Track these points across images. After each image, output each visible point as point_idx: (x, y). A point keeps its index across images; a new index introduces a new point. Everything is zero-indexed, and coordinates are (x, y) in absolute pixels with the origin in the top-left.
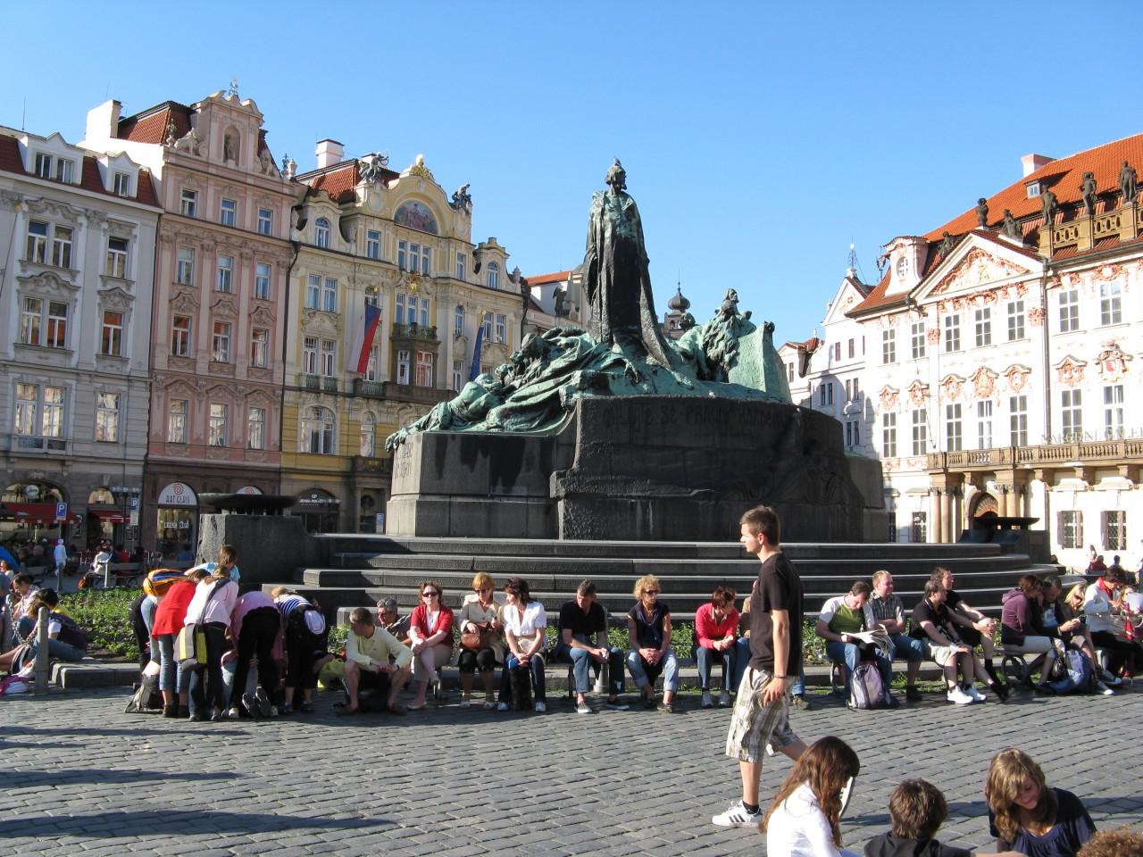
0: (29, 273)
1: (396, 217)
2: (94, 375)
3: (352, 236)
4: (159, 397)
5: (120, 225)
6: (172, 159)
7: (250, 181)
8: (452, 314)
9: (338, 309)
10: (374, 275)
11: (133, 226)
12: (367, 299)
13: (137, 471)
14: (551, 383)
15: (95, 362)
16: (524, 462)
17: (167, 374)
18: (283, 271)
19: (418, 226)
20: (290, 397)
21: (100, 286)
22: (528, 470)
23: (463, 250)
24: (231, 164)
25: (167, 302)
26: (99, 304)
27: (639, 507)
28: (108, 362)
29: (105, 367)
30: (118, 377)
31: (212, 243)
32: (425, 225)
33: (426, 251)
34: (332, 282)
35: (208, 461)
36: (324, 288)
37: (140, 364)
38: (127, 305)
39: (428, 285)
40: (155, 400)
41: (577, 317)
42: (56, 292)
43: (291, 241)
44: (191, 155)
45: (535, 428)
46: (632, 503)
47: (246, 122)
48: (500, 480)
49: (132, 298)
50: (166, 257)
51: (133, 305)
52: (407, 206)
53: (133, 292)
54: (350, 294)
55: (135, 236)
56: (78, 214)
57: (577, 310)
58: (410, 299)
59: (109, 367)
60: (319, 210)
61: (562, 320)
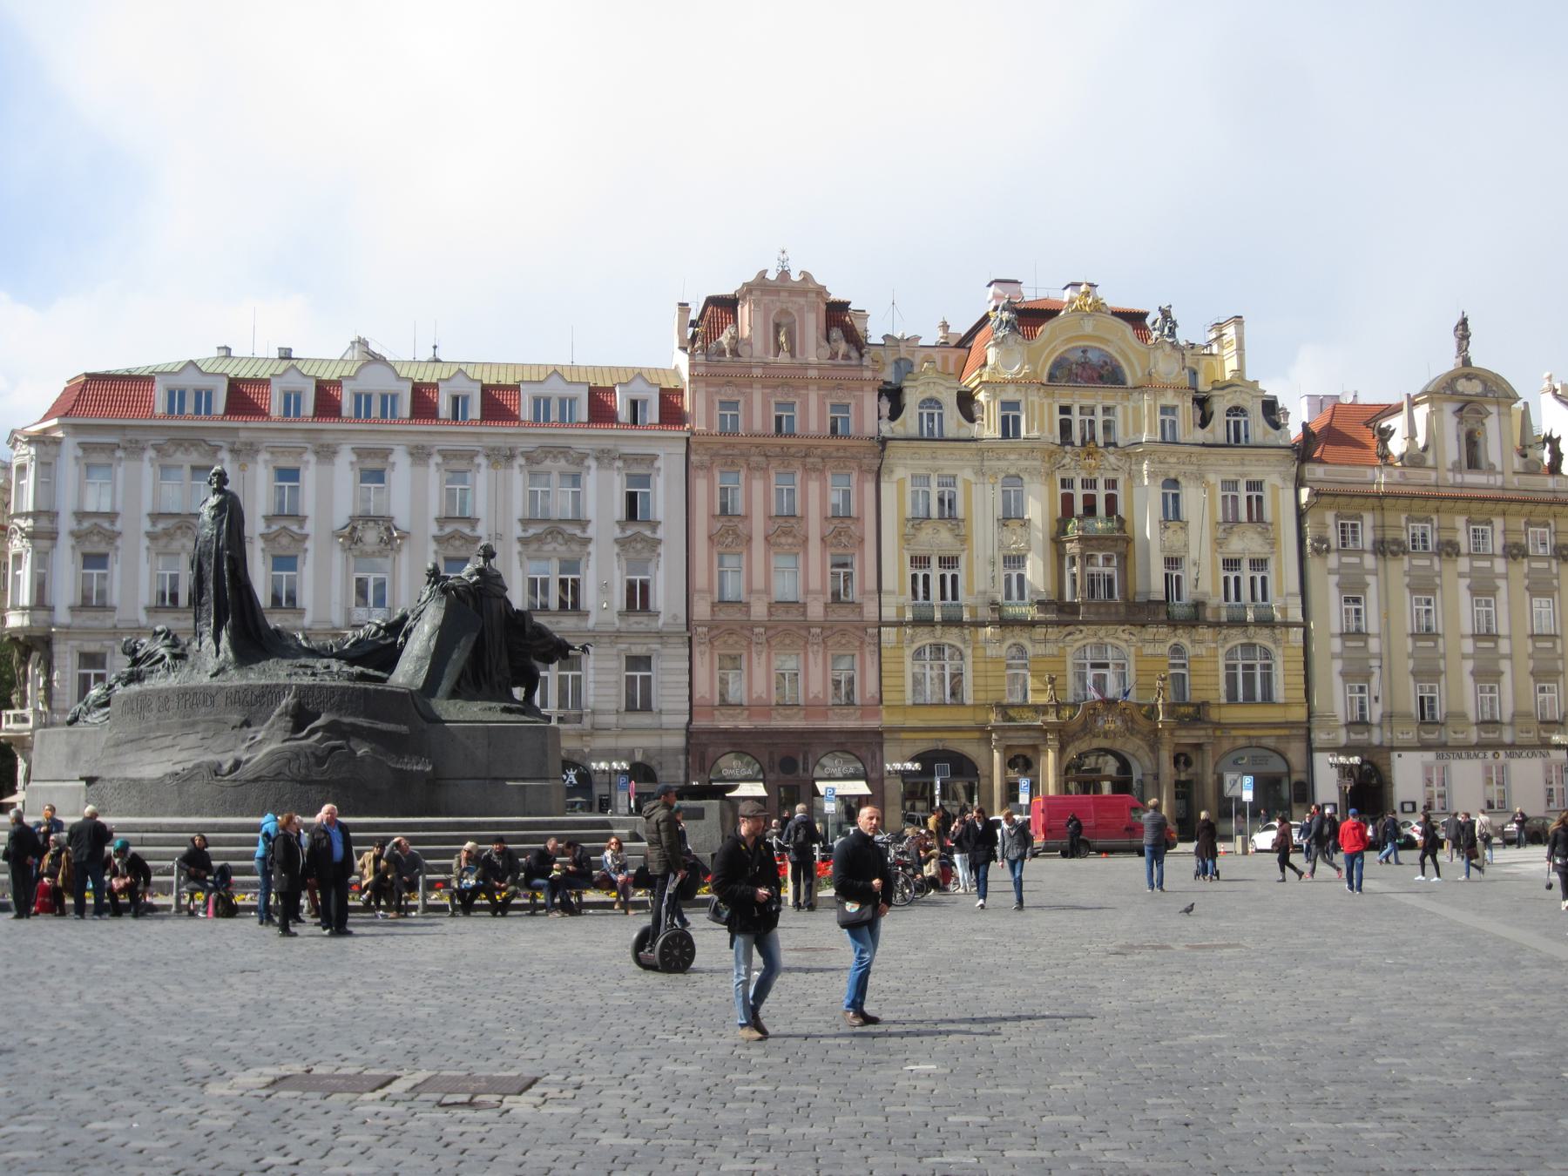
0: (531, 532)
1: (1051, 377)
2: (617, 635)
3: (978, 415)
4: (702, 654)
6: (701, 370)
7: (813, 373)
9: (960, 511)
10: (1012, 463)
11: (654, 457)
13: (679, 741)
15: (616, 621)
17: (713, 626)
18: (871, 478)
19: (1091, 380)
20: (889, 634)
21: (617, 533)
24: (784, 357)
28: (633, 619)
30: (647, 634)
31: (761, 459)
32: (1108, 375)
33: (1106, 410)
37: (675, 617)
39: (1112, 459)
42: (564, 548)
47: (802, 301)
50: (701, 486)
51: (662, 549)
53: (660, 533)
54: (977, 491)
56: (583, 457)
59: (638, 622)
60: (921, 389)
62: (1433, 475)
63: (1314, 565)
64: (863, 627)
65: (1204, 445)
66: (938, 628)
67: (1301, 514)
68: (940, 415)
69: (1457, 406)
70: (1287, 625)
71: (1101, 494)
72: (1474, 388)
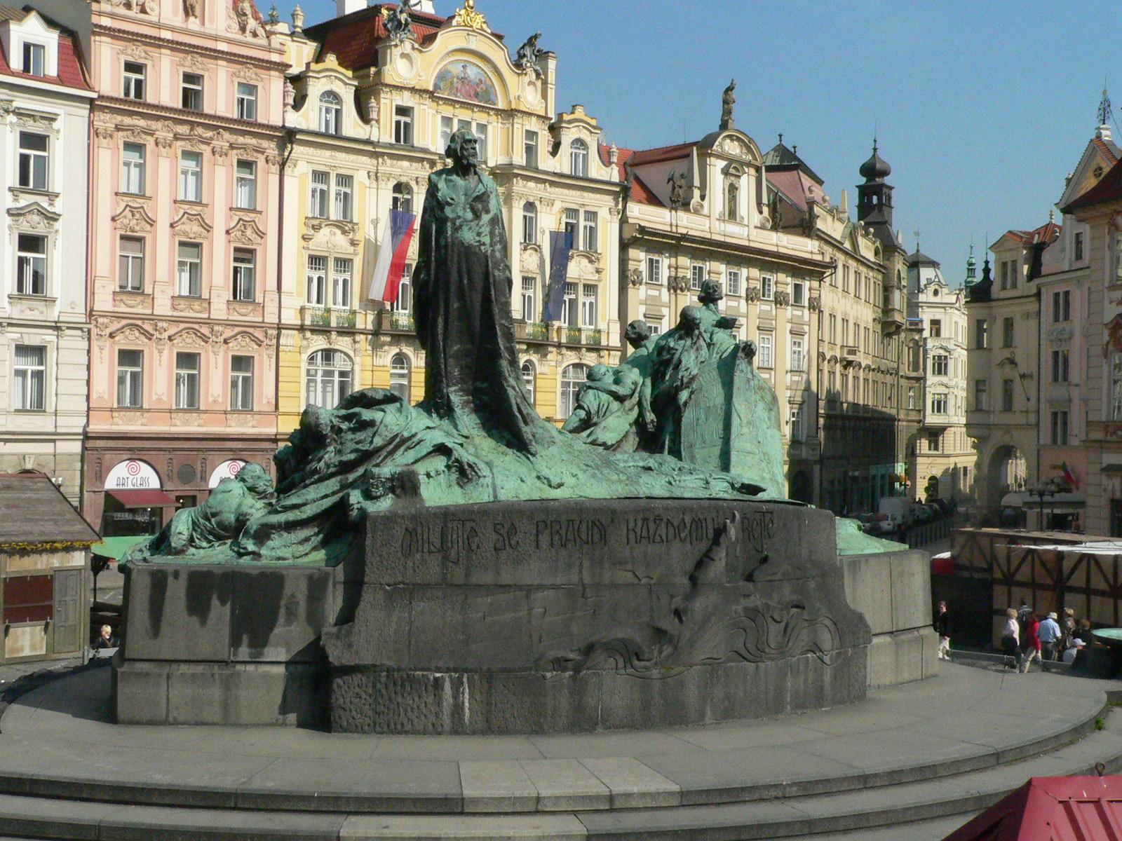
1: (436, 86)
3: (374, 115)
5: (31, 115)
6: (105, 22)
7: (222, 46)
11: (51, 119)
12: (395, 200)
13: (76, 447)
14: (333, 484)
16: (282, 611)
18: (275, 169)
20: (290, 339)
21: (9, 201)
22: (289, 622)
23: (533, 124)
24: (193, 23)
26: (10, 227)
27: (447, 685)
28: (26, 304)
29: (22, 311)
34: (345, 180)
35: (174, 429)
36: (333, 188)
40: (95, 350)
41: (702, 206)
44: (134, 13)
45: (306, 554)
46: (436, 679)
48: (245, 638)
49: (52, 218)
50: (105, 157)
51: (57, 225)
52: (450, 68)
53: (58, 207)
55: (58, 131)
57: (703, 197)
61: (681, 214)
63: (631, 292)
64: (261, 326)
65: (555, 174)
67: (624, 246)
68: (338, 112)
69: (724, 163)
70: (609, 349)
72: (733, 148)
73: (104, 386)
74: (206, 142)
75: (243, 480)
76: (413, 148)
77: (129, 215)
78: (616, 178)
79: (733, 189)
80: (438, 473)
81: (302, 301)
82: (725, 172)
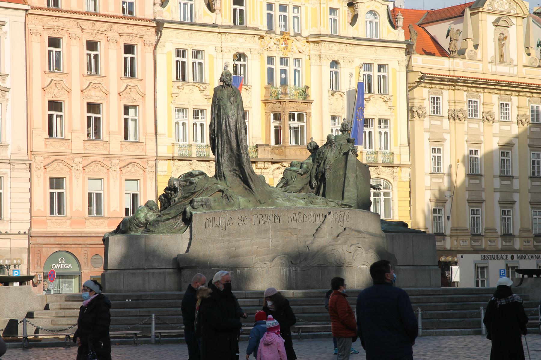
8: (326, 68)
13: (24, 243)
25: (40, 90)
31: (79, 31)
35: (87, 230)
36: (189, 60)
38: (4, 96)
39: (299, 44)
40: (34, 179)
43: (154, 20)
51: (8, 95)
53: (7, 84)
55: (6, 33)
57: (476, 47)
58: (281, 58)
62: (481, 65)
64: (144, 157)
66: (195, 161)
67: (410, 88)
69: (494, 18)
70: (400, 166)
71: (290, 68)
73: (42, 203)
74: (105, 33)
75: (148, 206)
76: (247, 28)
77: (54, 87)
78: (403, 39)
79: (502, 40)
80: (218, 199)
81: (173, 140)
82: (496, 23)
